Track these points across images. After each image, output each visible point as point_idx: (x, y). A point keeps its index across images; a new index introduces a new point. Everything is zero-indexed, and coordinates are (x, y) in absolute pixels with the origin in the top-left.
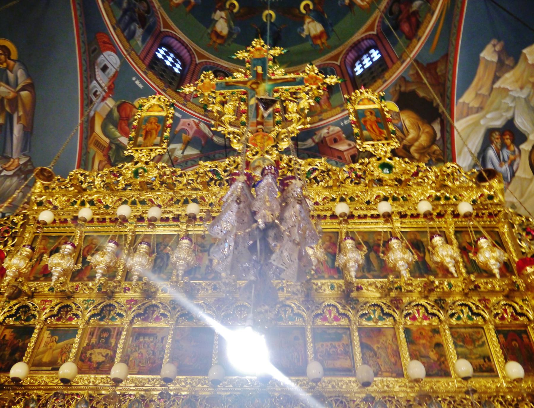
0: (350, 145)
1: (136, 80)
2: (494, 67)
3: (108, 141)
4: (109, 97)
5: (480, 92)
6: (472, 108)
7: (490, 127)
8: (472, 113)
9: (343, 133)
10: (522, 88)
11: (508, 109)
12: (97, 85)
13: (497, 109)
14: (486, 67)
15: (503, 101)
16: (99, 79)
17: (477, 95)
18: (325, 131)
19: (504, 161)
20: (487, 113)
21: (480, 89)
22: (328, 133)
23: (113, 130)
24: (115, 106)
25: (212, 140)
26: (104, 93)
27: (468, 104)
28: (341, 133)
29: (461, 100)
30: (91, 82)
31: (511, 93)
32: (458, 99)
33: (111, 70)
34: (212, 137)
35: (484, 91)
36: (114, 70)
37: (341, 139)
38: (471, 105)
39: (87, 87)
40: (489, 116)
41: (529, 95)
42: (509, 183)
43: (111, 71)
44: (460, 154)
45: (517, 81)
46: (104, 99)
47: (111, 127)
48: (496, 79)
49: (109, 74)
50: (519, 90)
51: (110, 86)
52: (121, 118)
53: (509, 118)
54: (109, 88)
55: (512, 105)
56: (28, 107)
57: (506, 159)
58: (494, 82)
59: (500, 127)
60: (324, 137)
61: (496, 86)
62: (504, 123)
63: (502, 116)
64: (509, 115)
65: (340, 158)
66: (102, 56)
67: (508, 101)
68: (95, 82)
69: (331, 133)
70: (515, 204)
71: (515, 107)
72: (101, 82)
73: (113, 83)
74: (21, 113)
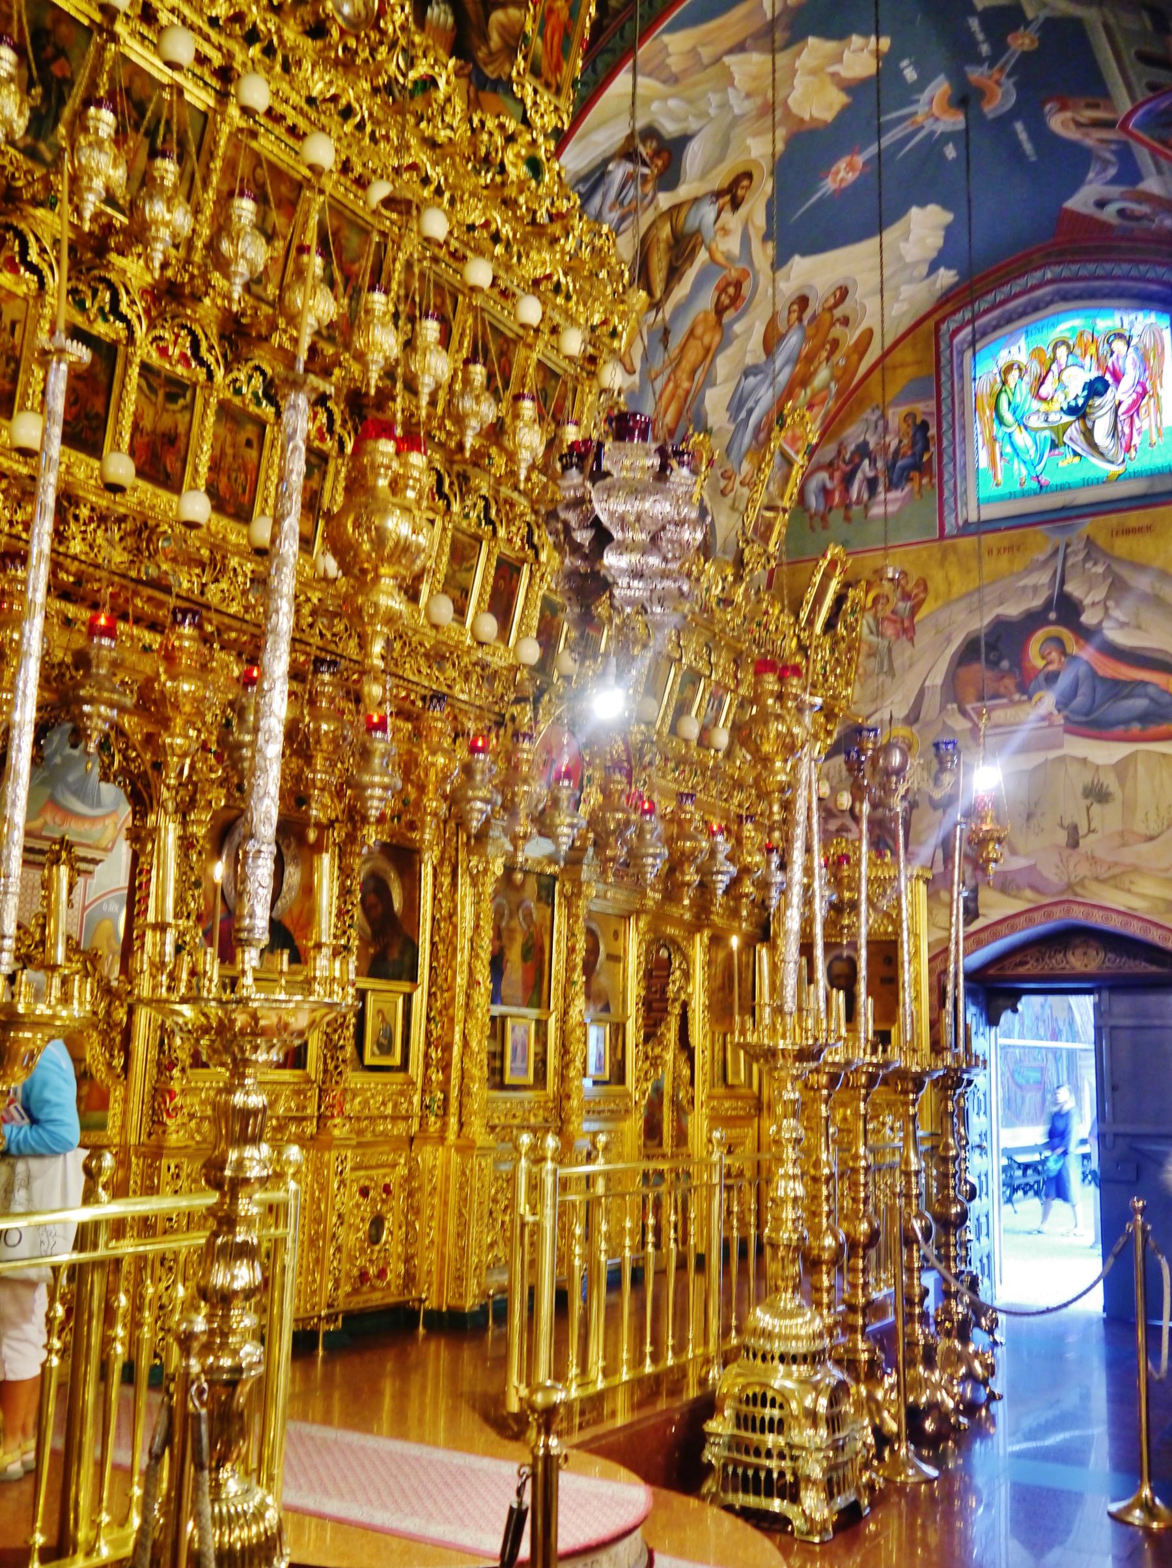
2: (756, 24)
5: (700, 49)
6: (668, 66)
7: (657, 125)
8: (657, 79)
10: (748, 96)
11: (703, 115)
13: (690, 101)
14: (748, 16)
15: (710, 95)
17: (693, 52)
19: (622, 203)
20: (672, 96)
21: (704, 45)
27: (669, 55)
29: (666, 38)
31: (730, 90)
32: (663, 32)
35: (706, 53)
38: (669, 61)
40: (672, 103)
41: (742, 116)
45: (755, 78)
48: (740, 48)
50: (743, 95)
53: (689, 132)
55: (712, 111)
57: (626, 202)
58: (731, 51)
59: (667, 136)
61: (727, 60)
62: (676, 135)
63: (686, 119)
64: (693, 125)
67: (715, 99)
71: (711, 119)
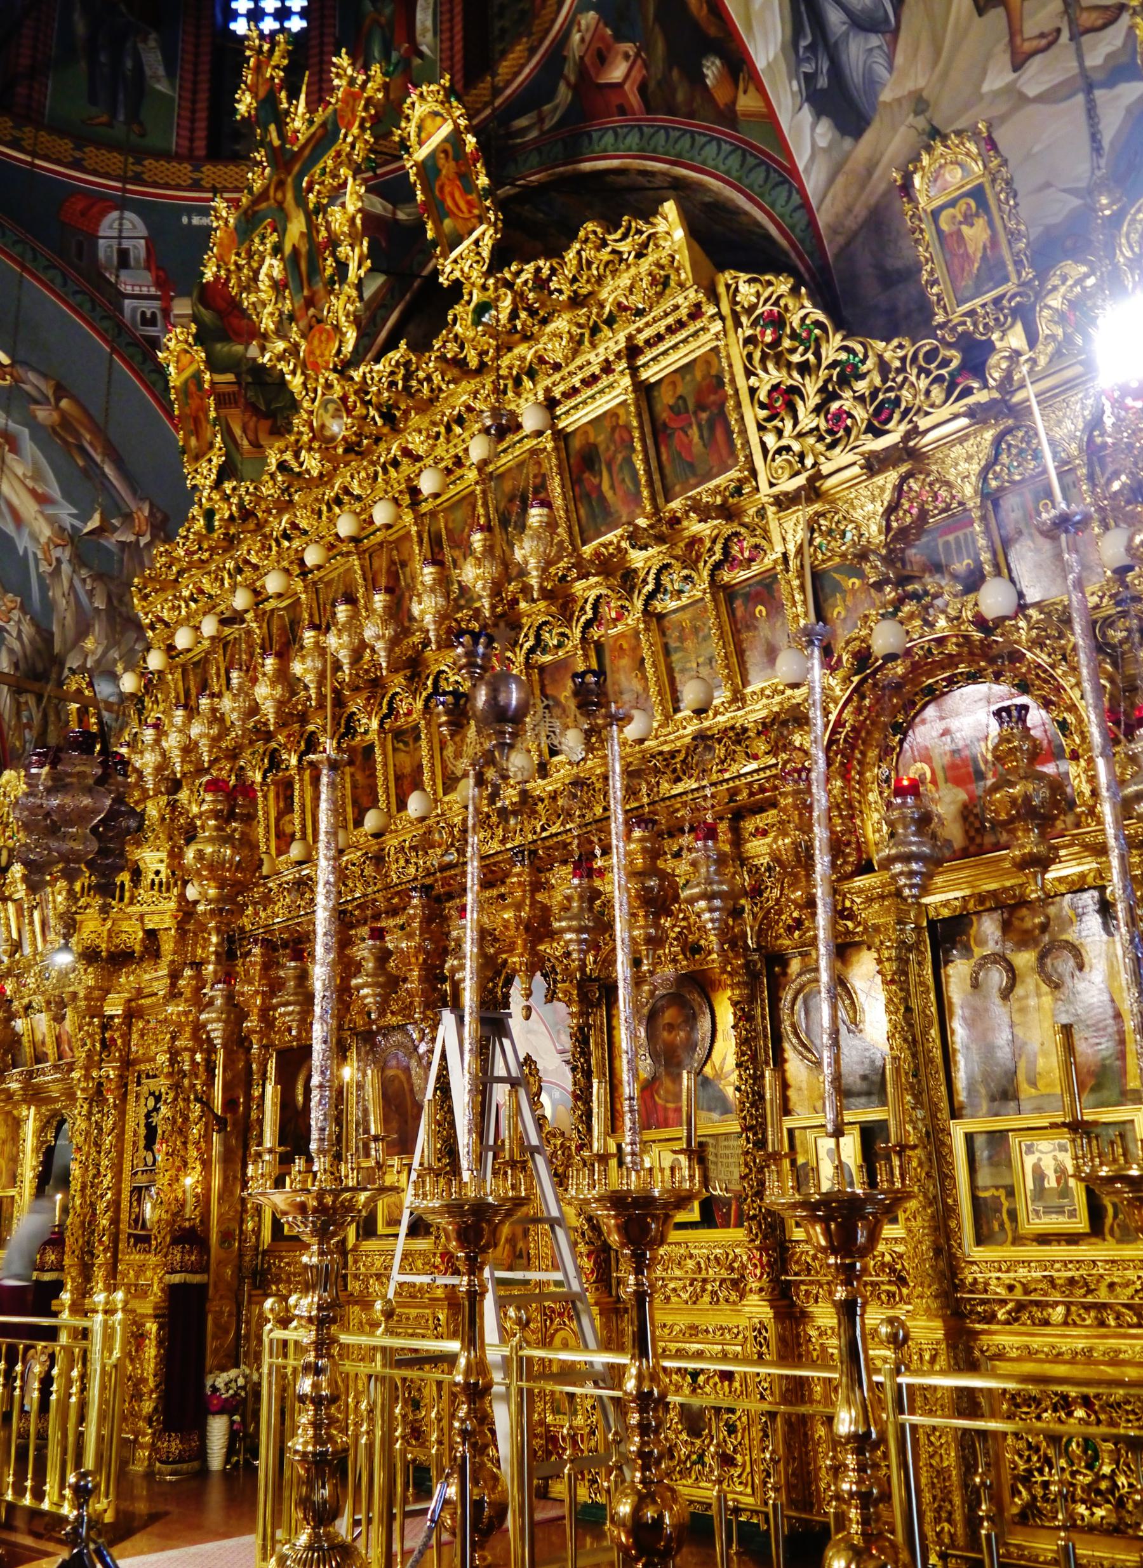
0: (626, 56)
1: (190, 219)
3: (230, 377)
4: (172, 298)
9: (606, 25)
12: (135, 302)
16: (128, 289)
18: (577, 37)
22: (582, 40)
23: (226, 349)
24: (193, 305)
25: (396, 221)
26: (157, 304)
28: (601, 25)
30: (121, 310)
33: (135, 247)
34: (394, 214)
36: (143, 242)
37: (609, 48)
39: (120, 326)
42: (896, 32)
43: (138, 248)
44: (749, 28)
46: (166, 312)
47: (219, 346)
49: (137, 260)
51: (158, 277)
52: (220, 314)
54: (158, 284)
56: (85, 421)
60: (581, 58)
65: (622, 110)
66: (101, 241)
68: (127, 301)
69: (588, 38)
70: (925, 94)
72: (137, 290)
73: (158, 268)
74: (88, 437)
